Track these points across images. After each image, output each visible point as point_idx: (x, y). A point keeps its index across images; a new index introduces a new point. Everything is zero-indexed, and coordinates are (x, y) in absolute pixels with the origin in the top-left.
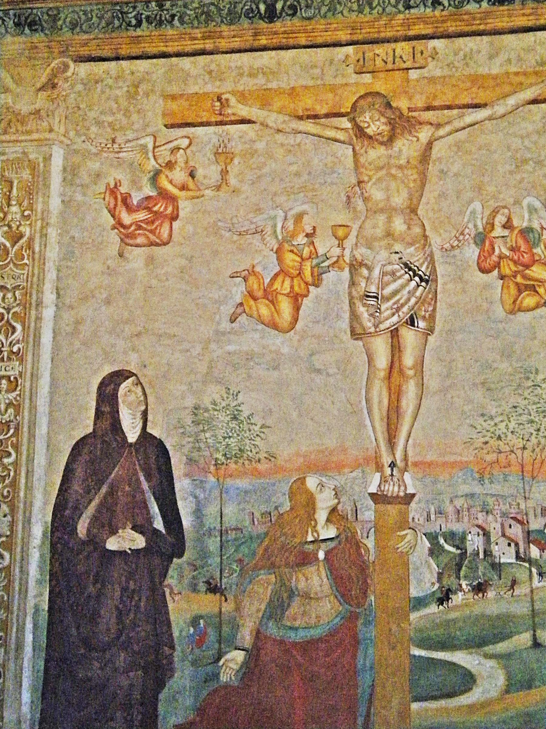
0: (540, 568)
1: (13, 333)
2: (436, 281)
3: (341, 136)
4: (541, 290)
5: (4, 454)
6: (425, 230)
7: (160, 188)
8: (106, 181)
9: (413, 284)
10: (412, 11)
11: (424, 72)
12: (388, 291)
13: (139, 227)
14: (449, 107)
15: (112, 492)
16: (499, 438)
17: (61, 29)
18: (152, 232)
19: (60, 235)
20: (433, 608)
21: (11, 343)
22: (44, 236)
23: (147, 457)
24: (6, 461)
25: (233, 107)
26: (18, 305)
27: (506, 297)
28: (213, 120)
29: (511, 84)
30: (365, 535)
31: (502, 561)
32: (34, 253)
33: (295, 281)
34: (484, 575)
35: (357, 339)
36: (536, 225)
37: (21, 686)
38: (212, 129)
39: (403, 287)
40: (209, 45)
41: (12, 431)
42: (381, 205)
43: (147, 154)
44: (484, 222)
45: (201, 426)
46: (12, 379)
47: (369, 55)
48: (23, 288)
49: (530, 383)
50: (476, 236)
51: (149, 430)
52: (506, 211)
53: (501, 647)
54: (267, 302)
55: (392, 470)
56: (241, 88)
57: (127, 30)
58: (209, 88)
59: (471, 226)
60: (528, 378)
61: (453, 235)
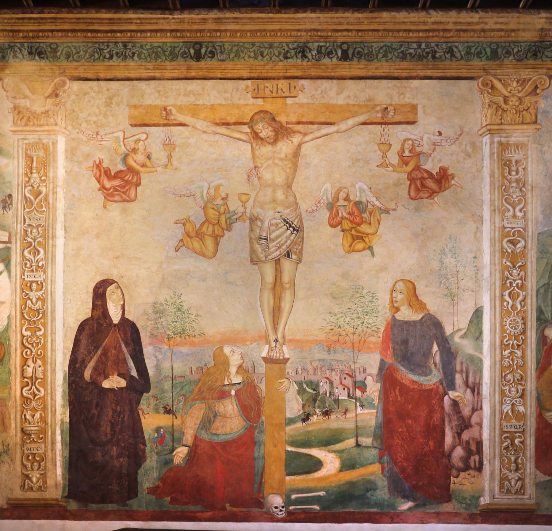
0: (361, 402)
1: (38, 254)
2: (303, 231)
3: (243, 137)
4: (366, 240)
5: (37, 329)
6: (296, 199)
7: (129, 165)
8: (94, 159)
9: (289, 232)
10: (289, 60)
11: (296, 100)
12: (273, 236)
13: (117, 190)
14: (312, 123)
16: (340, 327)
17: (60, 58)
18: (124, 193)
19: (65, 193)
21: (37, 261)
22: (55, 193)
23: (125, 334)
24: (38, 333)
25: (174, 115)
26: (40, 237)
27: (345, 243)
28: (161, 122)
29: (350, 111)
30: (260, 382)
31: (340, 398)
32: (49, 203)
33: (216, 227)
34: (329, 406)
35: (254, 264)
36: (364, 200)
37: (56, 465)
38: (161, 129)
39: (283, 234)
40: (157, 74)
41: (41, 315)
42: (269, 182)
43: (120, 143)
44: (333, 196)
45: (158, 314)
46: (39, 283)
47: (261, 87)
48: (43, 226)
49: (359, 295)
50: (327, 205)
51: (126, 316)
52: (346, 190)
54: (198, 239)
55: (276, 344)
56: (179, 103)
57: (104, 61)
58: (158, 102)
59: (324, 198)
60: (358, 292)
61: (314, 203)
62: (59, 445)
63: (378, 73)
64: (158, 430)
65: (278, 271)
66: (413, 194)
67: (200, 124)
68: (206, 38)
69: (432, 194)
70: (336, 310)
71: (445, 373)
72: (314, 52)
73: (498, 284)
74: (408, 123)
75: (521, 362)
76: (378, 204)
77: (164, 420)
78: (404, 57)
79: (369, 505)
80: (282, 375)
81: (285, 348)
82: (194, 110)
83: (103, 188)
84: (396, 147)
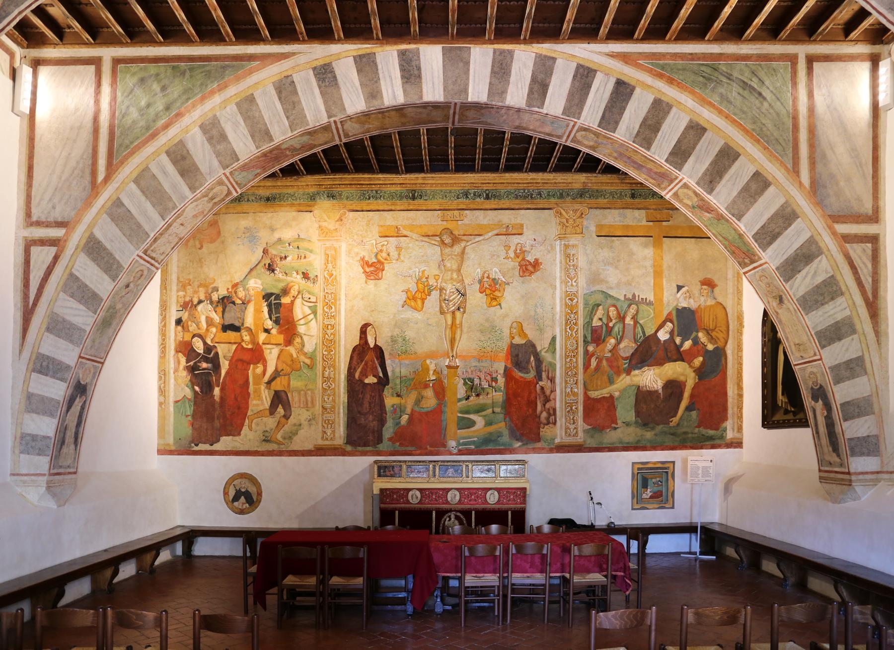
3: (436, 243)
12: (451, 298)
14: (471, 235)
15: (366, 364)
20: (464, 402)
40: (393, 208)
53: (484, 413)
58: (394, 223)
62: (342, 415)
63: (504, 207)
64: (393, 406)
65: (454, 318)
66: (521, 274)
67: (415, 236)
68: (418, 188)
69: (531, 273)
70: (483, 339)
71: (537, 372)
72: (472, 195)
73: (564, 322)
74: (519, 234)
75: (575, 365)
76: (504, 280)
77: (396, 400)
78: (517, 197)
79: (499, 445)
80: (456, 375)
81: (457, 360)
82: (412, 228)
83: (365, 272)
84: (513, 248)
